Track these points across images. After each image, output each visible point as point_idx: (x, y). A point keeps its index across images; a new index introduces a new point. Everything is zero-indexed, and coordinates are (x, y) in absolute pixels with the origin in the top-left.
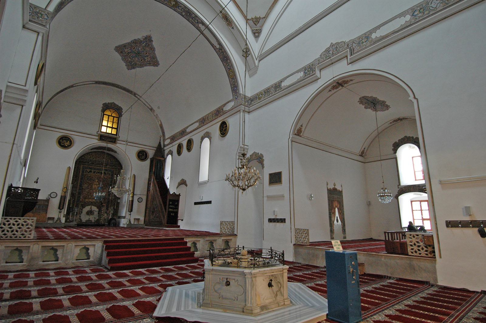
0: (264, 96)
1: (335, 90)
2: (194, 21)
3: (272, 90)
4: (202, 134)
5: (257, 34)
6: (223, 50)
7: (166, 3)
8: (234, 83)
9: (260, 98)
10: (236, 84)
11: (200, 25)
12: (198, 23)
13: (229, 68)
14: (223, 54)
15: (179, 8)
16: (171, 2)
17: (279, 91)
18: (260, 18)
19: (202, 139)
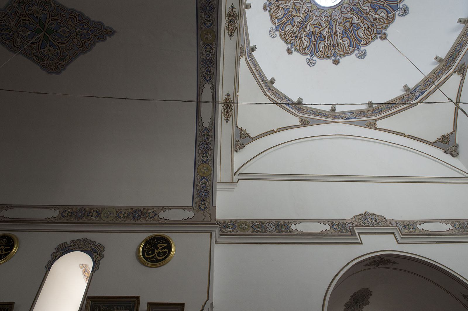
0: (251, 229)
1: (369, 267)
2: (206, 74)
3: (271, 227)
4: (68, 238)
5: (238, 148)
6: (212, 134)
7: (201, 28)
8: (203, 185)
9: (244, 229)
10: (209, 188)
11: (207, 86)
12: (208, 81)
13: (205, 160)
14: (208, 138)
15: (208, 48)
16: (209, 34)
17: (287, 234)
18: (248, 135)
19: (64, 249)
